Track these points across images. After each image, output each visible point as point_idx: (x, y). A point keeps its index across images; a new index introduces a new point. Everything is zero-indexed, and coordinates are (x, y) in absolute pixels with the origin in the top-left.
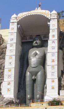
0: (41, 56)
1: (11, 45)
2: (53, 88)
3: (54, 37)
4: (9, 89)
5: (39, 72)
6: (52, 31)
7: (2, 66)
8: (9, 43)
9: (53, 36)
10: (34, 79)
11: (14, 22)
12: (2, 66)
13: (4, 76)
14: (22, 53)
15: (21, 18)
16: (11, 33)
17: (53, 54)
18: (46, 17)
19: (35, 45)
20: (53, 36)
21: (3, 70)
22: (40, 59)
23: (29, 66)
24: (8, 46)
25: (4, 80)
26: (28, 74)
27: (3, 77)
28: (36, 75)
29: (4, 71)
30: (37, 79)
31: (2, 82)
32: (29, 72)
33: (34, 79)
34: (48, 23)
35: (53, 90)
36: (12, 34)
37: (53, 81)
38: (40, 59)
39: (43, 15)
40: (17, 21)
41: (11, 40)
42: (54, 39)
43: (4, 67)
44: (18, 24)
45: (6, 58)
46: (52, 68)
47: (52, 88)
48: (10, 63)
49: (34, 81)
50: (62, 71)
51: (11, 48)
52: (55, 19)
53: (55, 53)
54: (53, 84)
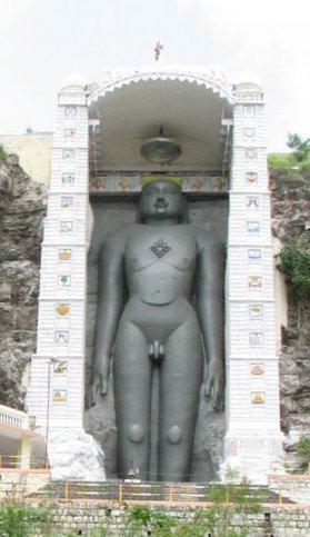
1: (67, 202)
2: (258, 401)
3: (252, 181)
4: (63, 394)
6: (246, 154)
7: (24, 289)
8: (57, 194)
9: (249, 177)
10: (156, 357)
11: (75, 106)
12: (25, 289)
13: (39, 336)
14: (91, 242)
15: (108, 89)
16: (65, 150)
17: (252, 253)
18: (218, 93)
19: (153, 210)
20: (249, 177)
21: (31, 308)
22: (180, 274)
23: (131, 300)
25: (35, 352)
26: (132, 333)
28: (164, 342)
29: (34, 313)
30: (167, 358)
31: (30, 360)
32: (135, 323)
33: (156, 357)
34: (225, 122)
35: (258, 410)
36: (66, 153)
37: (258, 372)
38: (180, 274)
40: (89, 103)
41: (63, 180)
42: (252, 188)
43: (35, 295)
44: (92, 116)
45: (43, 257)
46: (254, 314)
47: (254, 402)
49: (157, 363)
50: (283, 328)
51: (67, 214)
52: (254, 105)
54: (259, 384)
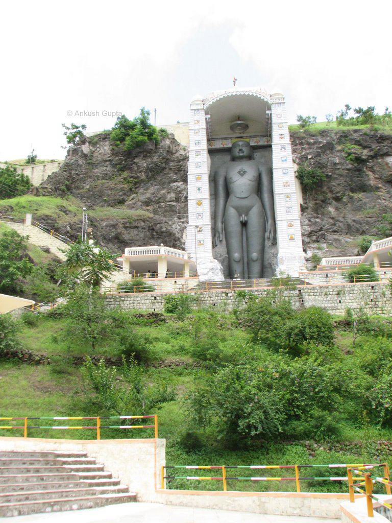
0: (254, 176)
2: (292, 239)
3: (282, 138)
4: (202, 242)
5: (252, 207)
7: (181, 195)
10: (244, 222)
11: (198, 110)
16: (195, 130)
17: (284, 171)
19: (237, 154)
20: (280, 136)
21: (184, 204)
22: (252, 183)
24: (192, 156)
25: (188, 223)
26: (232, 212)
27: (187, 217)
28: (247, 215)
29: (186, 206)
30: (249, 222)
31: (186, 227)
32: (233, 207)
33: (244, 222)
35: (292, 243)
36: (196, 131)
37: (291, 225)
38: (252, 183)
39: (260, 97)
40: (205, 108)
42: (282, 141)
43: (186, 197)
44: (206, 113)
46: (287, 199)
47: (290, 240)
48: (199, 189)
49: (244, 224)
50: (301, 205)
51: (198, 159)
53: (289, 169)
54: (291, 231)
